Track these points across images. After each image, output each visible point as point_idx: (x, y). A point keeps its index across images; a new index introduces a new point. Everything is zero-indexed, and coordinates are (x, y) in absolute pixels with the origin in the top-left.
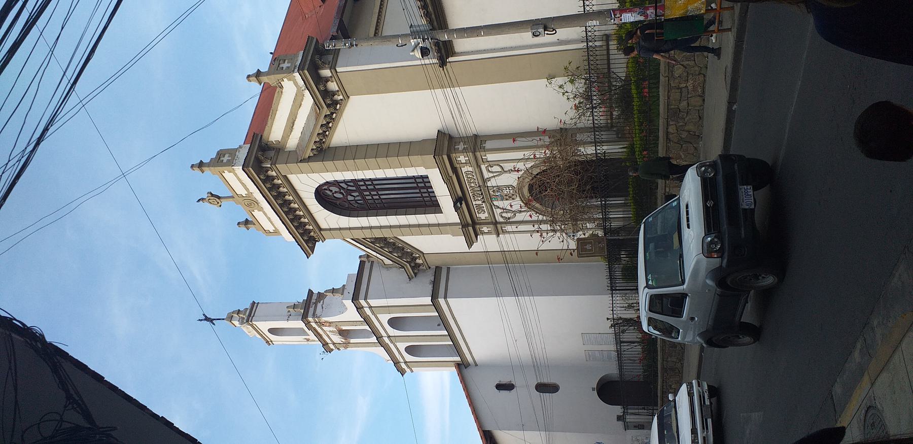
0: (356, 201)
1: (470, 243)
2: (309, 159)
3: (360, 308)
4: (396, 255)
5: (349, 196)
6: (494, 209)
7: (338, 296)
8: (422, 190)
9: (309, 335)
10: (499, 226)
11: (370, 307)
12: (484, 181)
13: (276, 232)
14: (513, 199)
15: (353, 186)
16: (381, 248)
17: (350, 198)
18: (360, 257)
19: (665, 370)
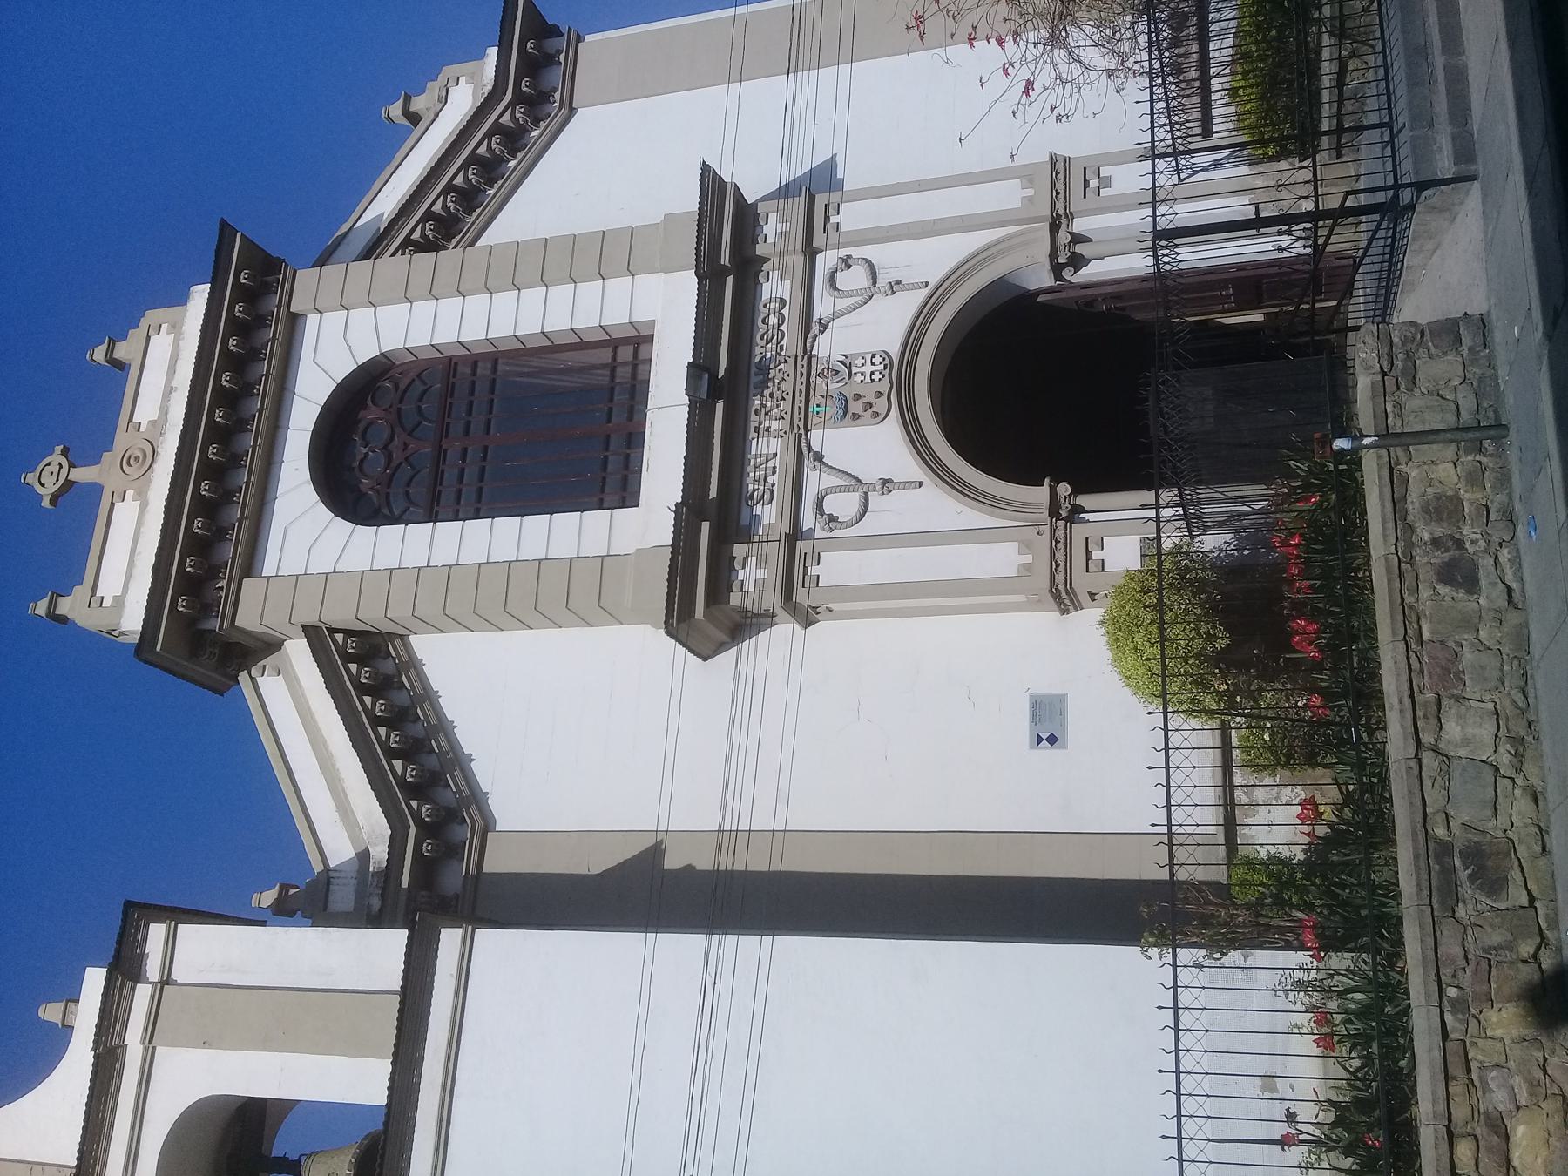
13: (119, 601)
14: (876, 414)
19: (1437, 854)
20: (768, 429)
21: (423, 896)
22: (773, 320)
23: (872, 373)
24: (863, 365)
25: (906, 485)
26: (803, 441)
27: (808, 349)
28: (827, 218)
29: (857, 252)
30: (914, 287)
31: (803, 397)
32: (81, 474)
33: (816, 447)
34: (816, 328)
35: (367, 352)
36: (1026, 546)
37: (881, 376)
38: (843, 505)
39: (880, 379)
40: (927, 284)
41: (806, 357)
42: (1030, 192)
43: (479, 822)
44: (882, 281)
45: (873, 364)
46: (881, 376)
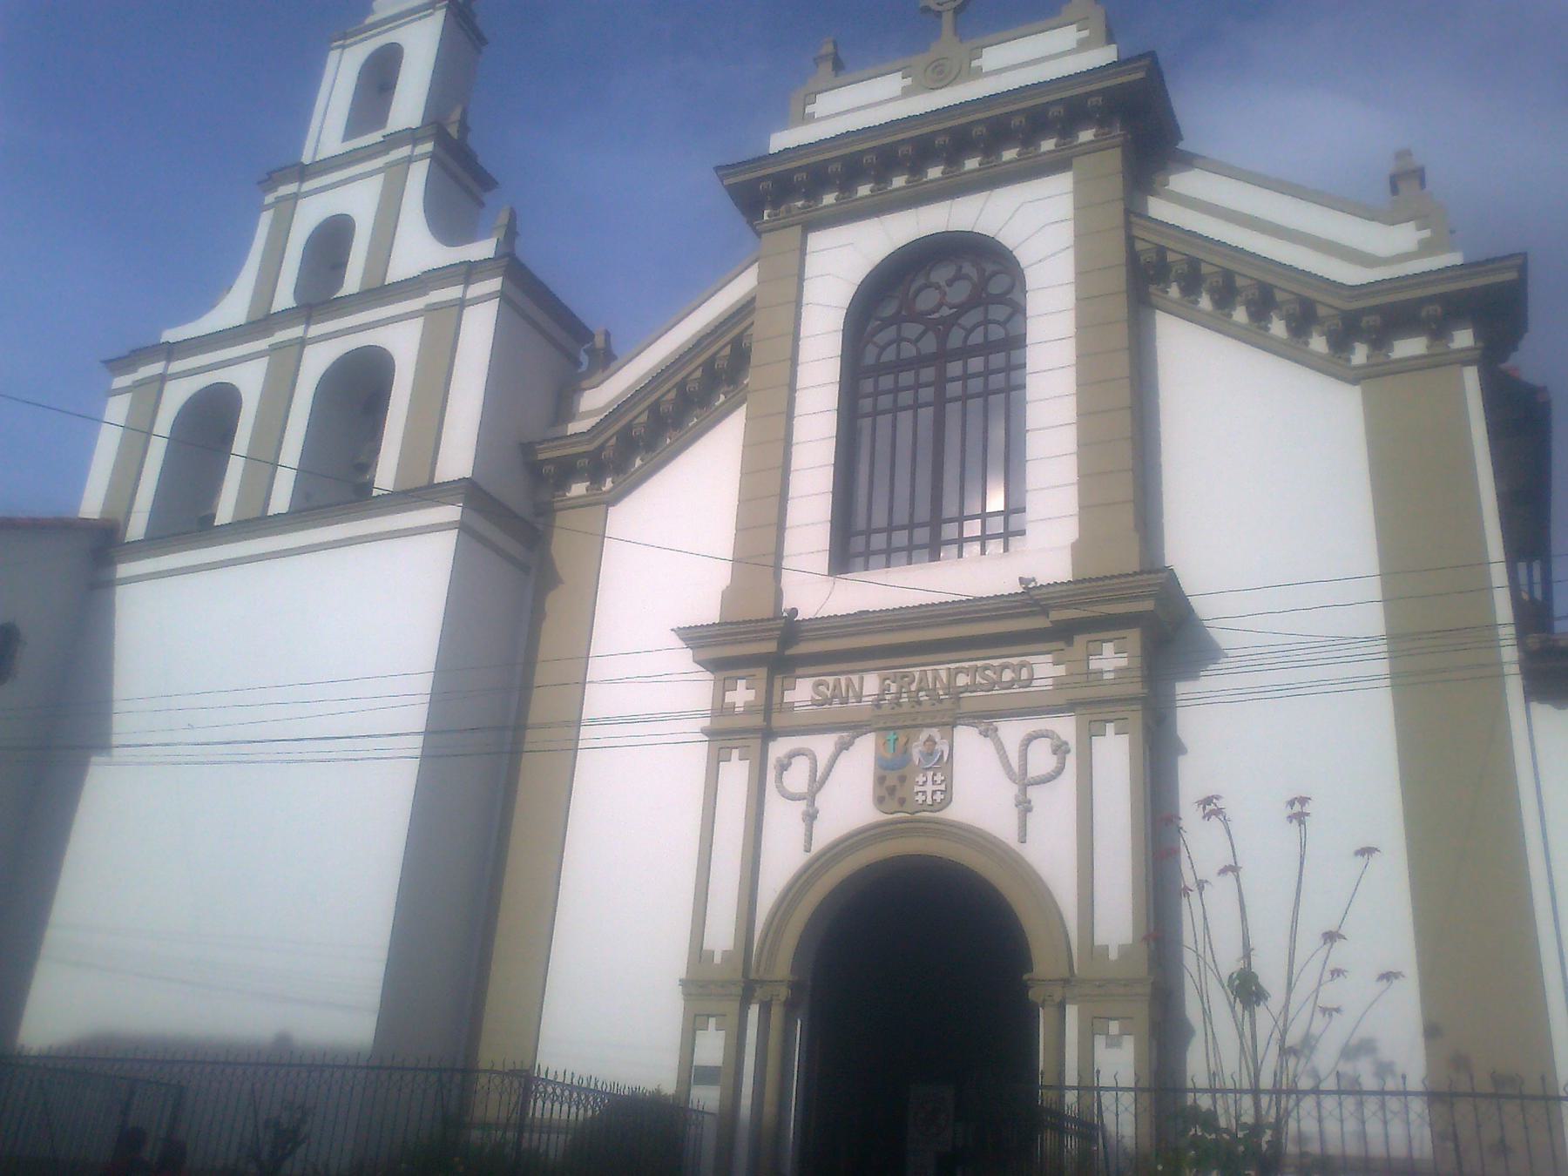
0: (899, 340)
1: (694, 637)
2: (1130, 239)
4: (637, 421)
5: (921, 328)
7: (501, 233)
8: (922, 535)
9: (343, 141)
11: (462, 304)
12: (986, 718)
13: (808, 119)
14: (880, 801)
15: (966, 338)
16: (681, 387)
17: (912, 330)
18: (607, 335)
22: (1007, 675)
23: (924, 793)
24: (934, 782)
29: (1071, 761)
32: (948, 19)
35: (1024, 256)
38: (797, 778)
44: (1034, 793)
45: (934, 792)
46: (920, 802)
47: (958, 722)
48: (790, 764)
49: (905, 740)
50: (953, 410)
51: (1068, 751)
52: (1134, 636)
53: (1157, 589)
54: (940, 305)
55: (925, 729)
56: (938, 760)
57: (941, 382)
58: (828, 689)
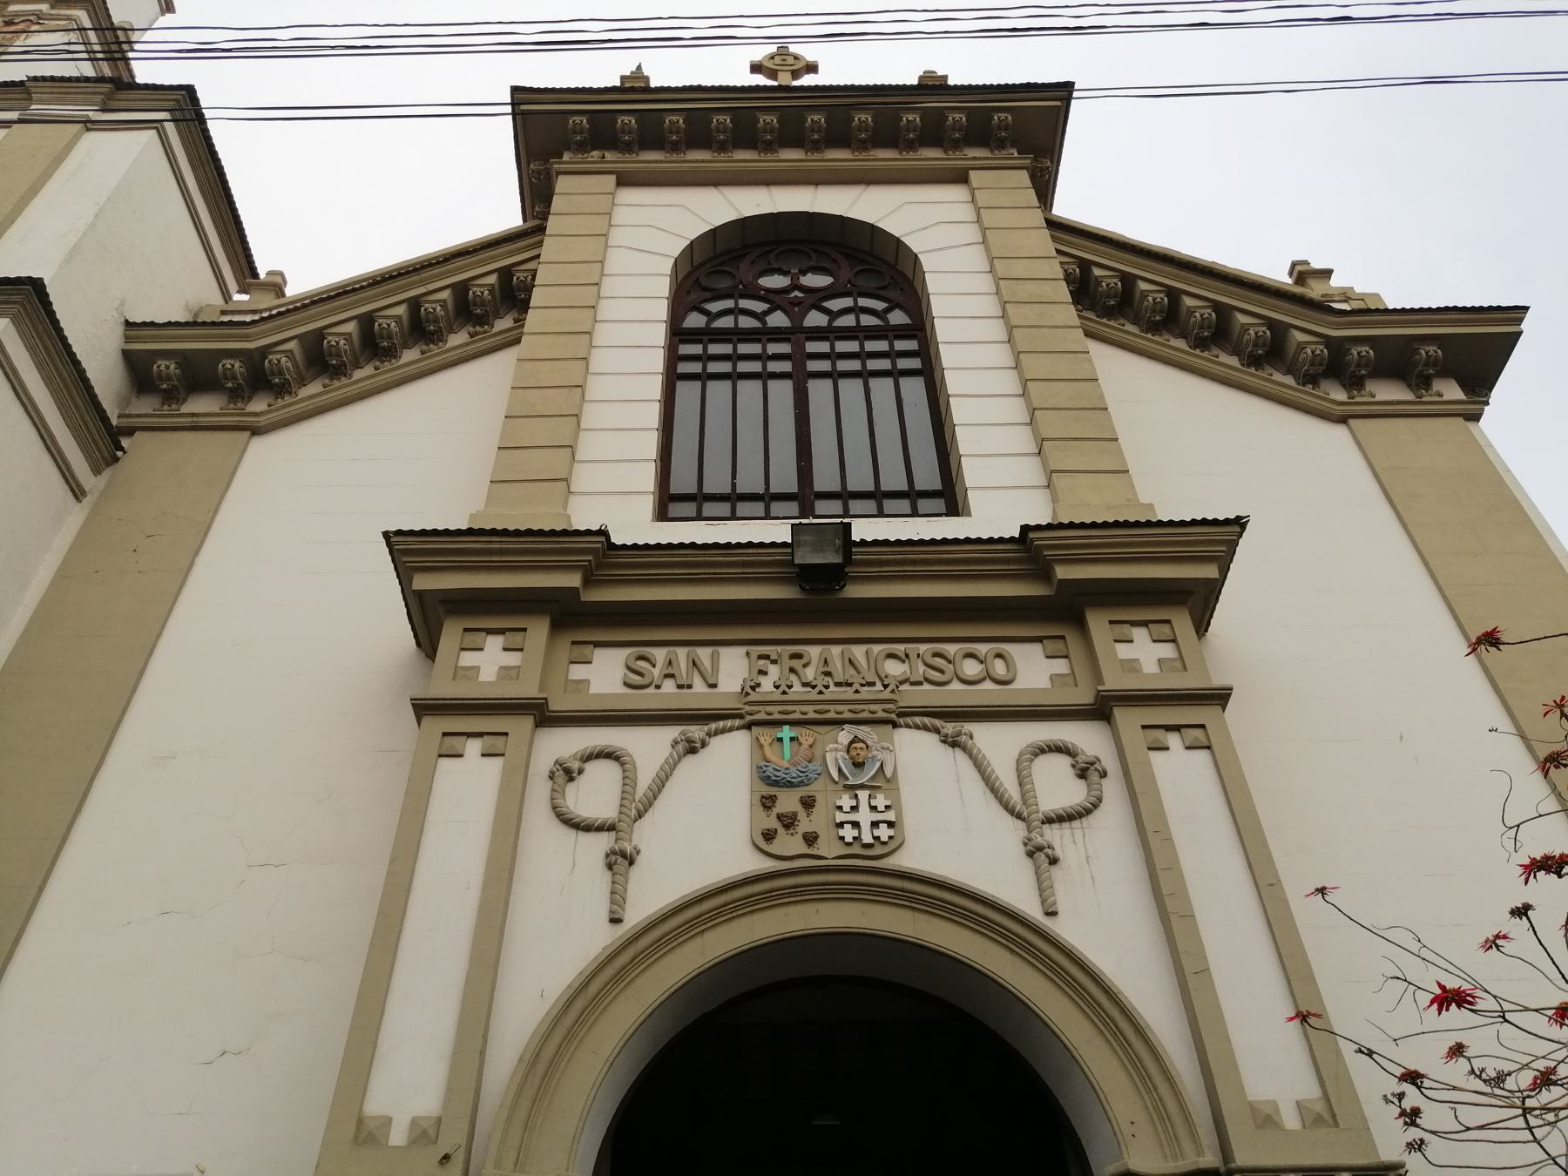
3: (109, 96)
6: (672, 732)
10: (519, 726)
14: (769, 836)
20: (763, 673)
21: (168, 367)
22: (971, 668)
23: (856, 825)
24: (873, 808)
25: (617, 898)
26: (729, 723)
27: (909, 720)
28: (1176, 728)
30: (1044, 891)
31: (812, 715)
33: (716, 743)
34: (949, 728)
36: (424, 1134)
37: (849, 839)
39: (842, 838)
40: (1052, 914)
41: (893, 716)
42: (1291, 1121)
43: (263, 421)
44: (1055, 836)
45: (875, 824)
46: (849, 839)
47: (901, 721)
48: (580, 772)
49: (811, 740)
50: (819, 392)
51: (1104, 774)
52: (1182, 622)
53: (1224, 549)
54: (796, 286)
55: (846, 727)
56: (873, 778)
57: (799, 358)
58: (654, 666)
